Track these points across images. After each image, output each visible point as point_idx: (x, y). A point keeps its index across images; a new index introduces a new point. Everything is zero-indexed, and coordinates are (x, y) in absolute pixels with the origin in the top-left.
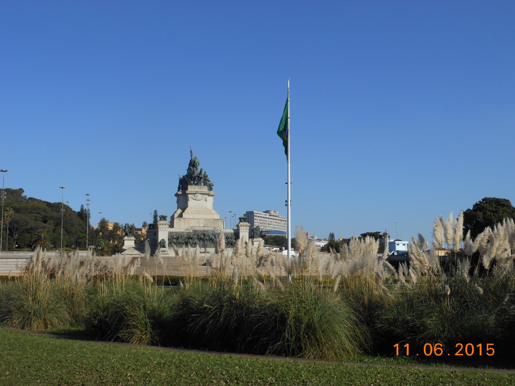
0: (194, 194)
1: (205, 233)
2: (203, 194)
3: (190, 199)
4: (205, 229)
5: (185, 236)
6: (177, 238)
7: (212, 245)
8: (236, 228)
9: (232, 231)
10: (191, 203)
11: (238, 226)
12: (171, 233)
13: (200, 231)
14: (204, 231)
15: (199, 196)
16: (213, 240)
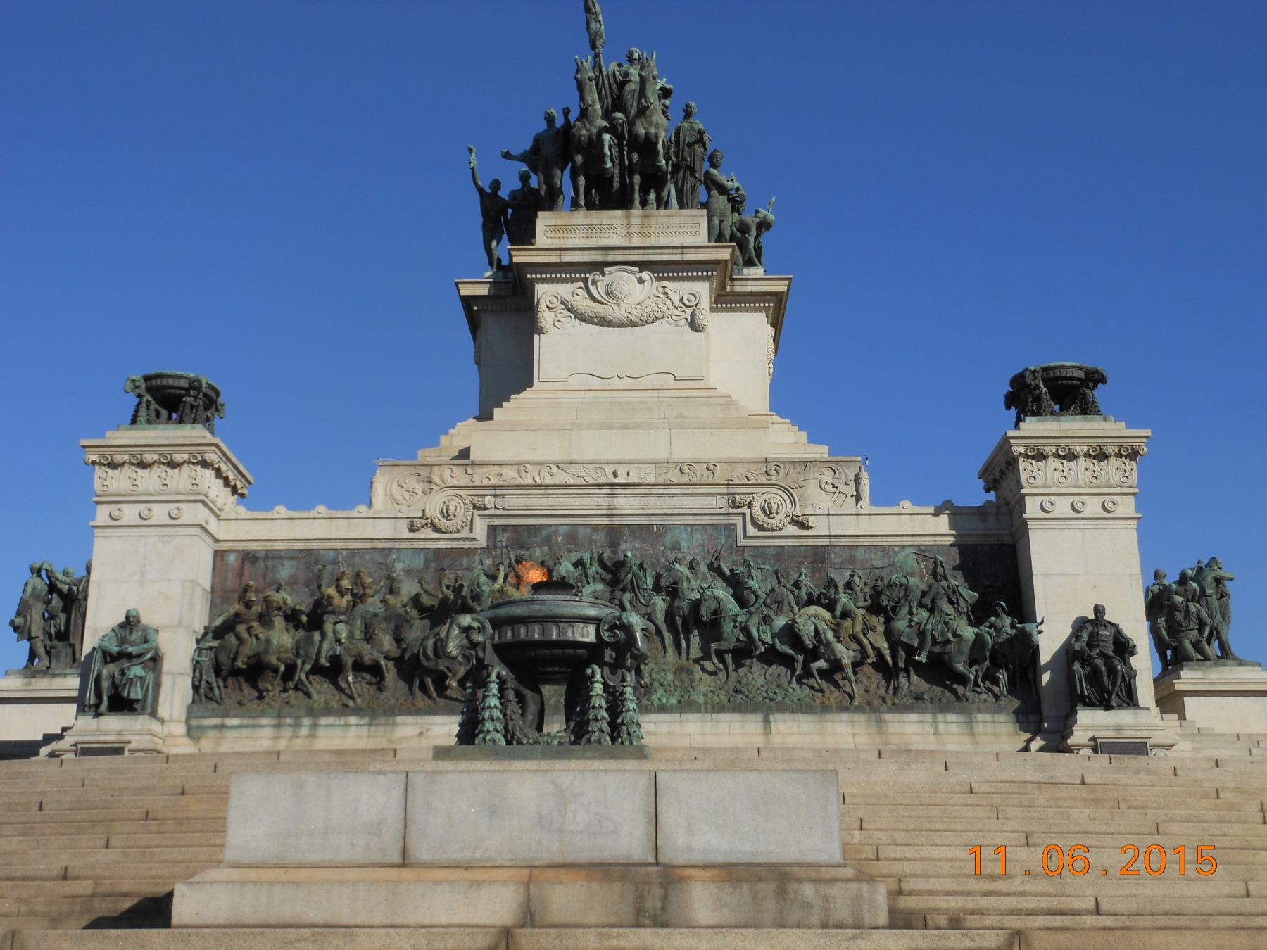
0: (585, 270)
1: (630, 551)
2: (663, 269)
3: (545, 317)
4: (626, 502)
5: (408, 588)
6: (315, 618)
7: (704, 684)
8: (976, 495)
9: (942, 525)
10: (560, 345)
11: (1001, 471)
12: (248, 557)
13: (573, 537)
14: (614, 534)
15: (635, 291)
16: (711, 629)
